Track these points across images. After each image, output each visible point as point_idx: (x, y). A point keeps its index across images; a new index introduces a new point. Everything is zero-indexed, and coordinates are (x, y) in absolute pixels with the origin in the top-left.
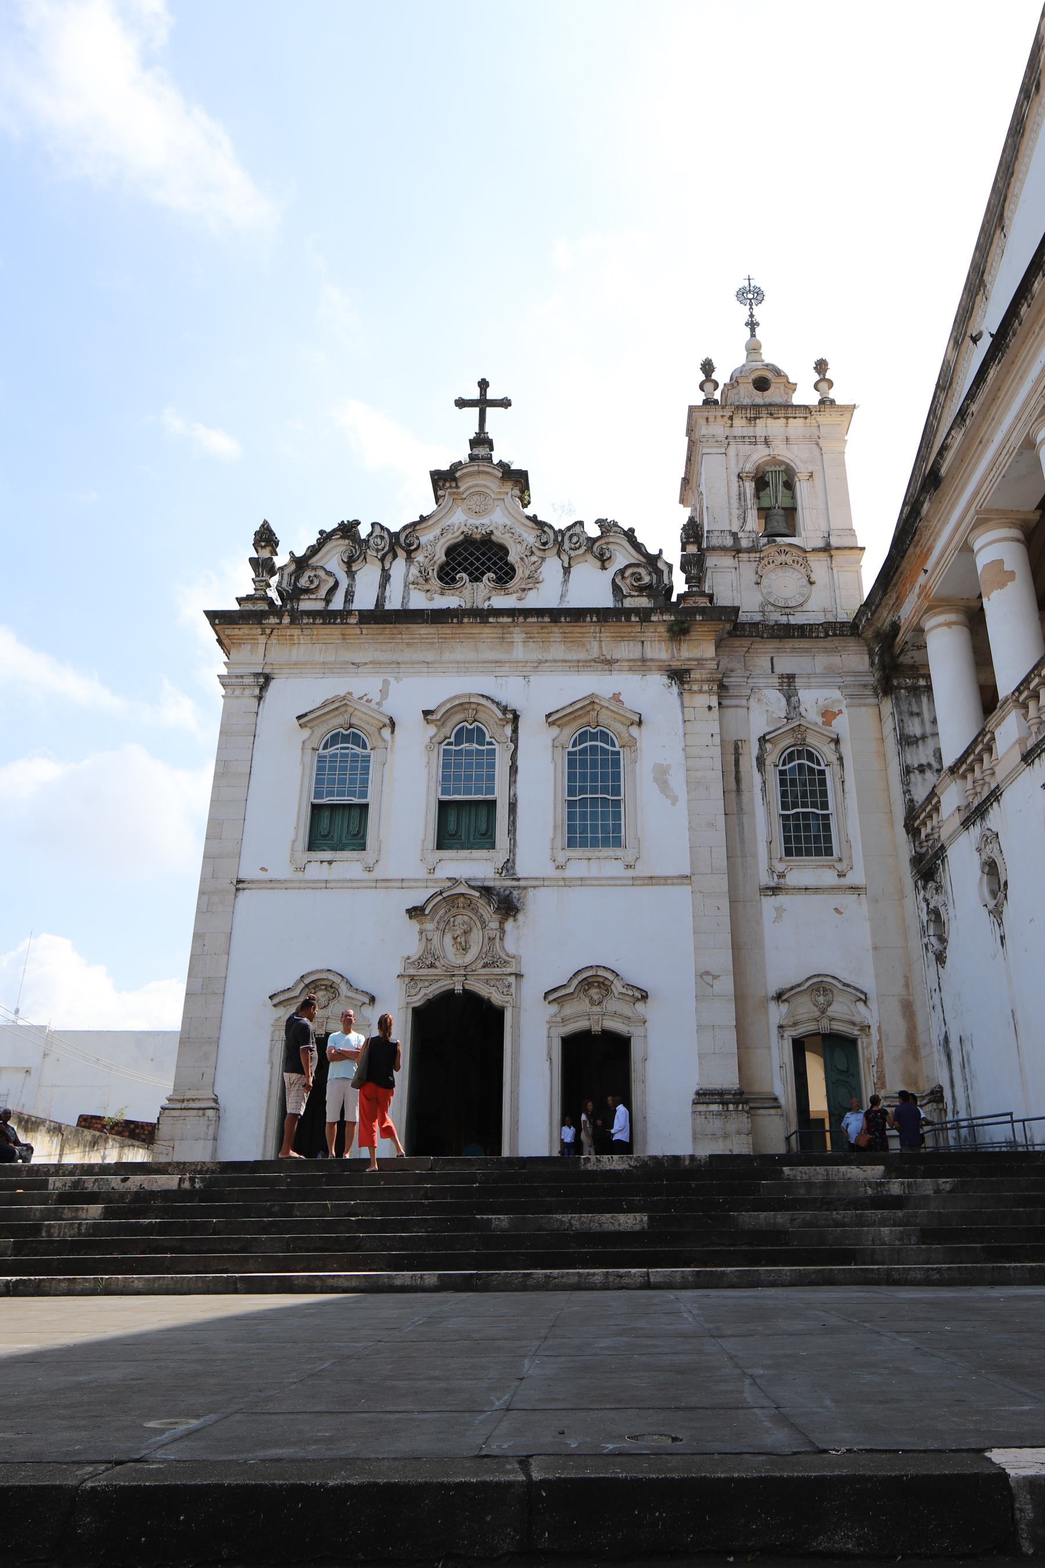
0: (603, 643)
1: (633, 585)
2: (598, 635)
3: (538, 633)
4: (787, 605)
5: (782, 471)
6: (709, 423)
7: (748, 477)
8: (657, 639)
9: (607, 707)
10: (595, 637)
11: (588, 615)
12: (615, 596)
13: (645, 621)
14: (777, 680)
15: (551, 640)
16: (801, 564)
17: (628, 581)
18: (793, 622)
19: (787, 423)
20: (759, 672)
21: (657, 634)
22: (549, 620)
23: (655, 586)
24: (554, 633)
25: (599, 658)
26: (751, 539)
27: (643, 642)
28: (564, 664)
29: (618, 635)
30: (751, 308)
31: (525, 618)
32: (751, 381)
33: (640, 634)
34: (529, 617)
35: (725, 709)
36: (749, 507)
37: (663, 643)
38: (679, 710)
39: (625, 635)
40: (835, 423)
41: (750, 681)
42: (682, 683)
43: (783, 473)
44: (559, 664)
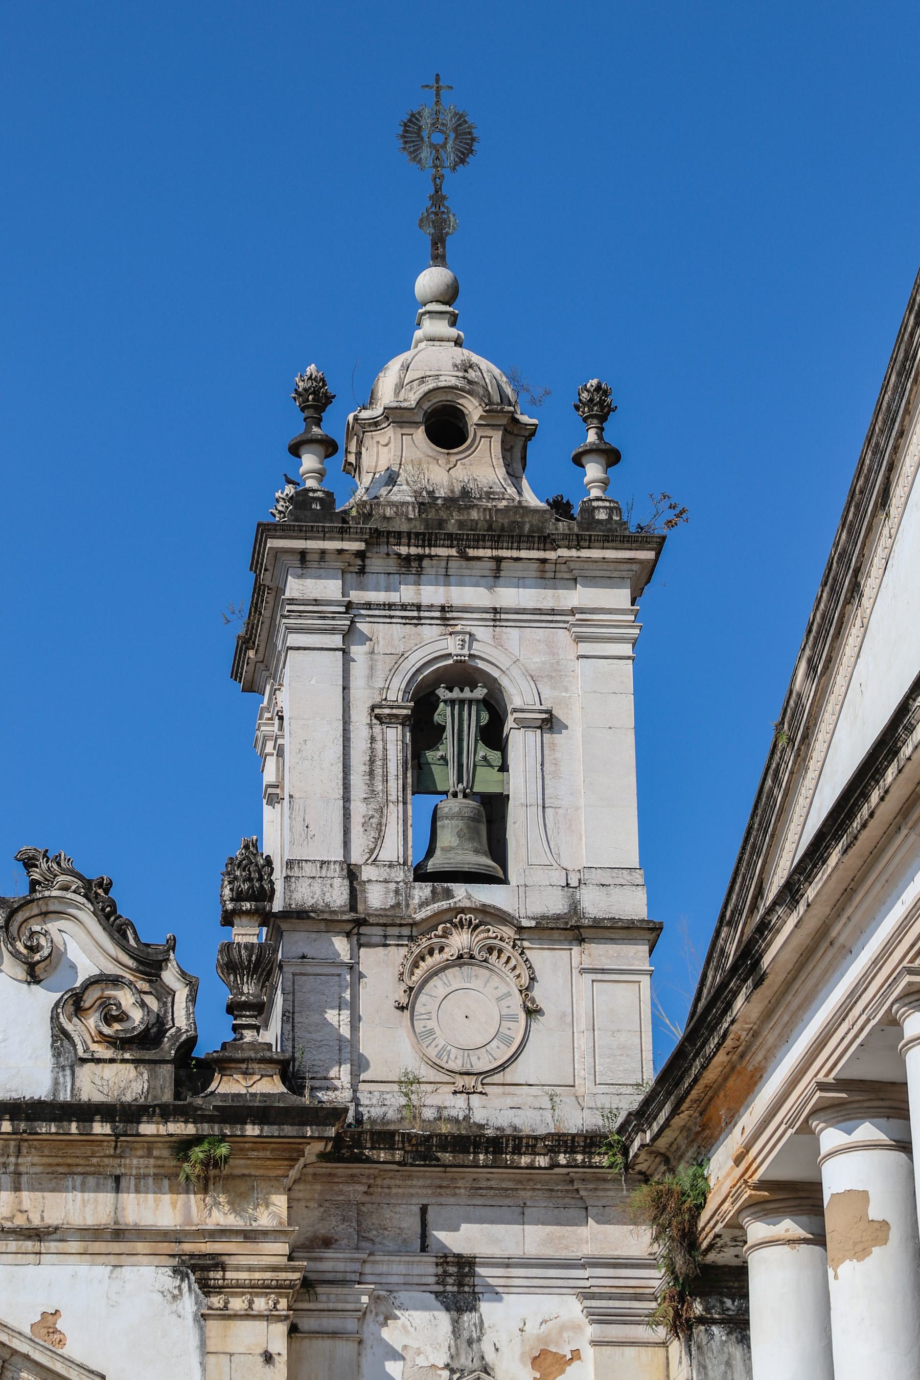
0: (24, 1179)
1: (101, 1033)
2: (12, 1159)
4: (467, 1068)
5: (478, 701)
6: (309, 564)
7: (396, 716)
8: (152, 1171)
12: (57, 1053)
14: (432, 1270)
16: (509, 958)
17: (93, 1021)
18: (479, 1117)
19: (498, 569)
20: (391, 1246)
21: (152, 1161)
23: (154, 1030)
25: (11, 1219)
26: (393, 886)
27: (117, 1179)
29: (60, 1160)
30: (438, 179)
32: (420, 418)
35: (306, 1343)
36: (393, 798)
37: (166, 1182)
38: (194, 1359)
39: (78, 1161)
40: (615, 574)
41: (368, 1269)
42: (207, 1288)
43: (482, 707)
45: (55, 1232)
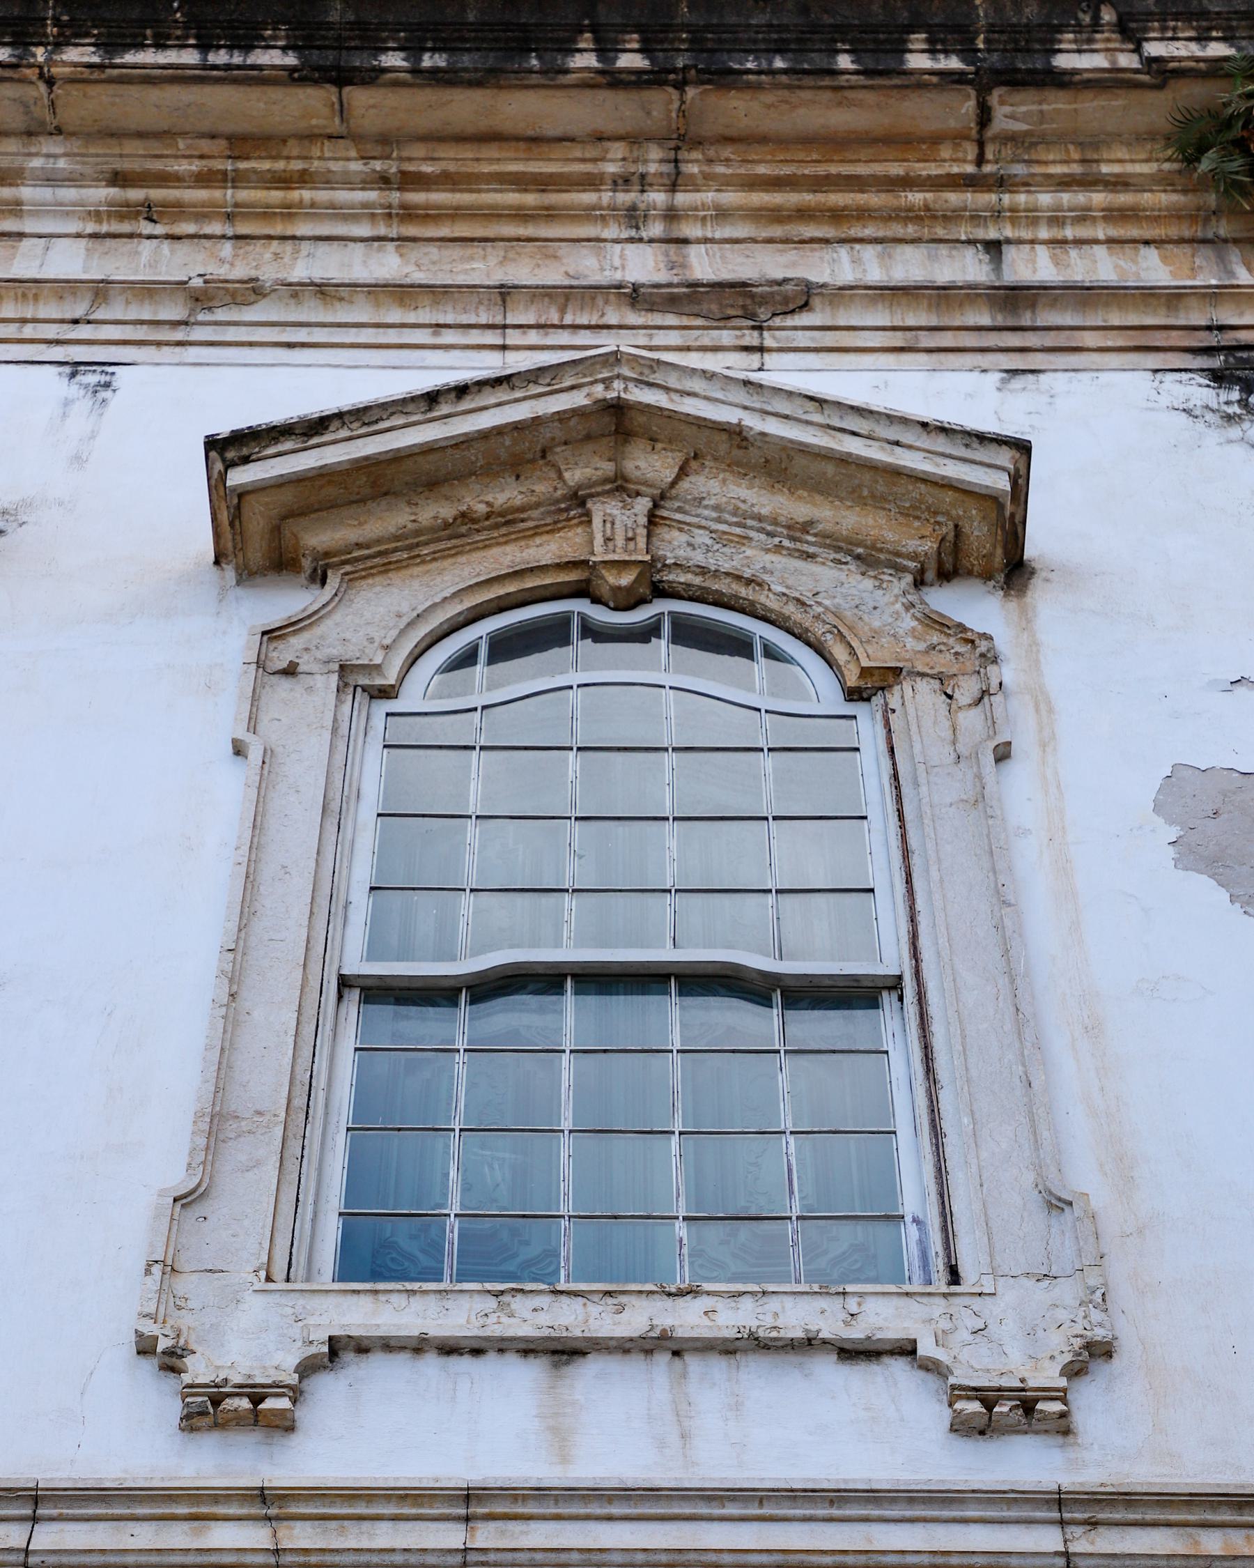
2: (658, 198)
3: (204, 179)
9: (736, 434)
10: (634, 217)
11: (586, 41)
13: (1015, 80)
15: (303, 229)
21: (1099, 198)
22: (291, 60)
24: (328, 181)
28: (395, 316)
29: (808, 198)
31: (111, 45)
33: (969, 198)
34: (141, 46)
44: (361, 312)
45: (805, 306)
